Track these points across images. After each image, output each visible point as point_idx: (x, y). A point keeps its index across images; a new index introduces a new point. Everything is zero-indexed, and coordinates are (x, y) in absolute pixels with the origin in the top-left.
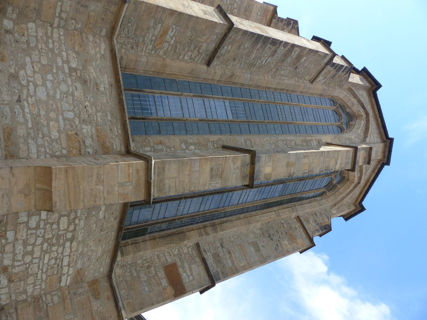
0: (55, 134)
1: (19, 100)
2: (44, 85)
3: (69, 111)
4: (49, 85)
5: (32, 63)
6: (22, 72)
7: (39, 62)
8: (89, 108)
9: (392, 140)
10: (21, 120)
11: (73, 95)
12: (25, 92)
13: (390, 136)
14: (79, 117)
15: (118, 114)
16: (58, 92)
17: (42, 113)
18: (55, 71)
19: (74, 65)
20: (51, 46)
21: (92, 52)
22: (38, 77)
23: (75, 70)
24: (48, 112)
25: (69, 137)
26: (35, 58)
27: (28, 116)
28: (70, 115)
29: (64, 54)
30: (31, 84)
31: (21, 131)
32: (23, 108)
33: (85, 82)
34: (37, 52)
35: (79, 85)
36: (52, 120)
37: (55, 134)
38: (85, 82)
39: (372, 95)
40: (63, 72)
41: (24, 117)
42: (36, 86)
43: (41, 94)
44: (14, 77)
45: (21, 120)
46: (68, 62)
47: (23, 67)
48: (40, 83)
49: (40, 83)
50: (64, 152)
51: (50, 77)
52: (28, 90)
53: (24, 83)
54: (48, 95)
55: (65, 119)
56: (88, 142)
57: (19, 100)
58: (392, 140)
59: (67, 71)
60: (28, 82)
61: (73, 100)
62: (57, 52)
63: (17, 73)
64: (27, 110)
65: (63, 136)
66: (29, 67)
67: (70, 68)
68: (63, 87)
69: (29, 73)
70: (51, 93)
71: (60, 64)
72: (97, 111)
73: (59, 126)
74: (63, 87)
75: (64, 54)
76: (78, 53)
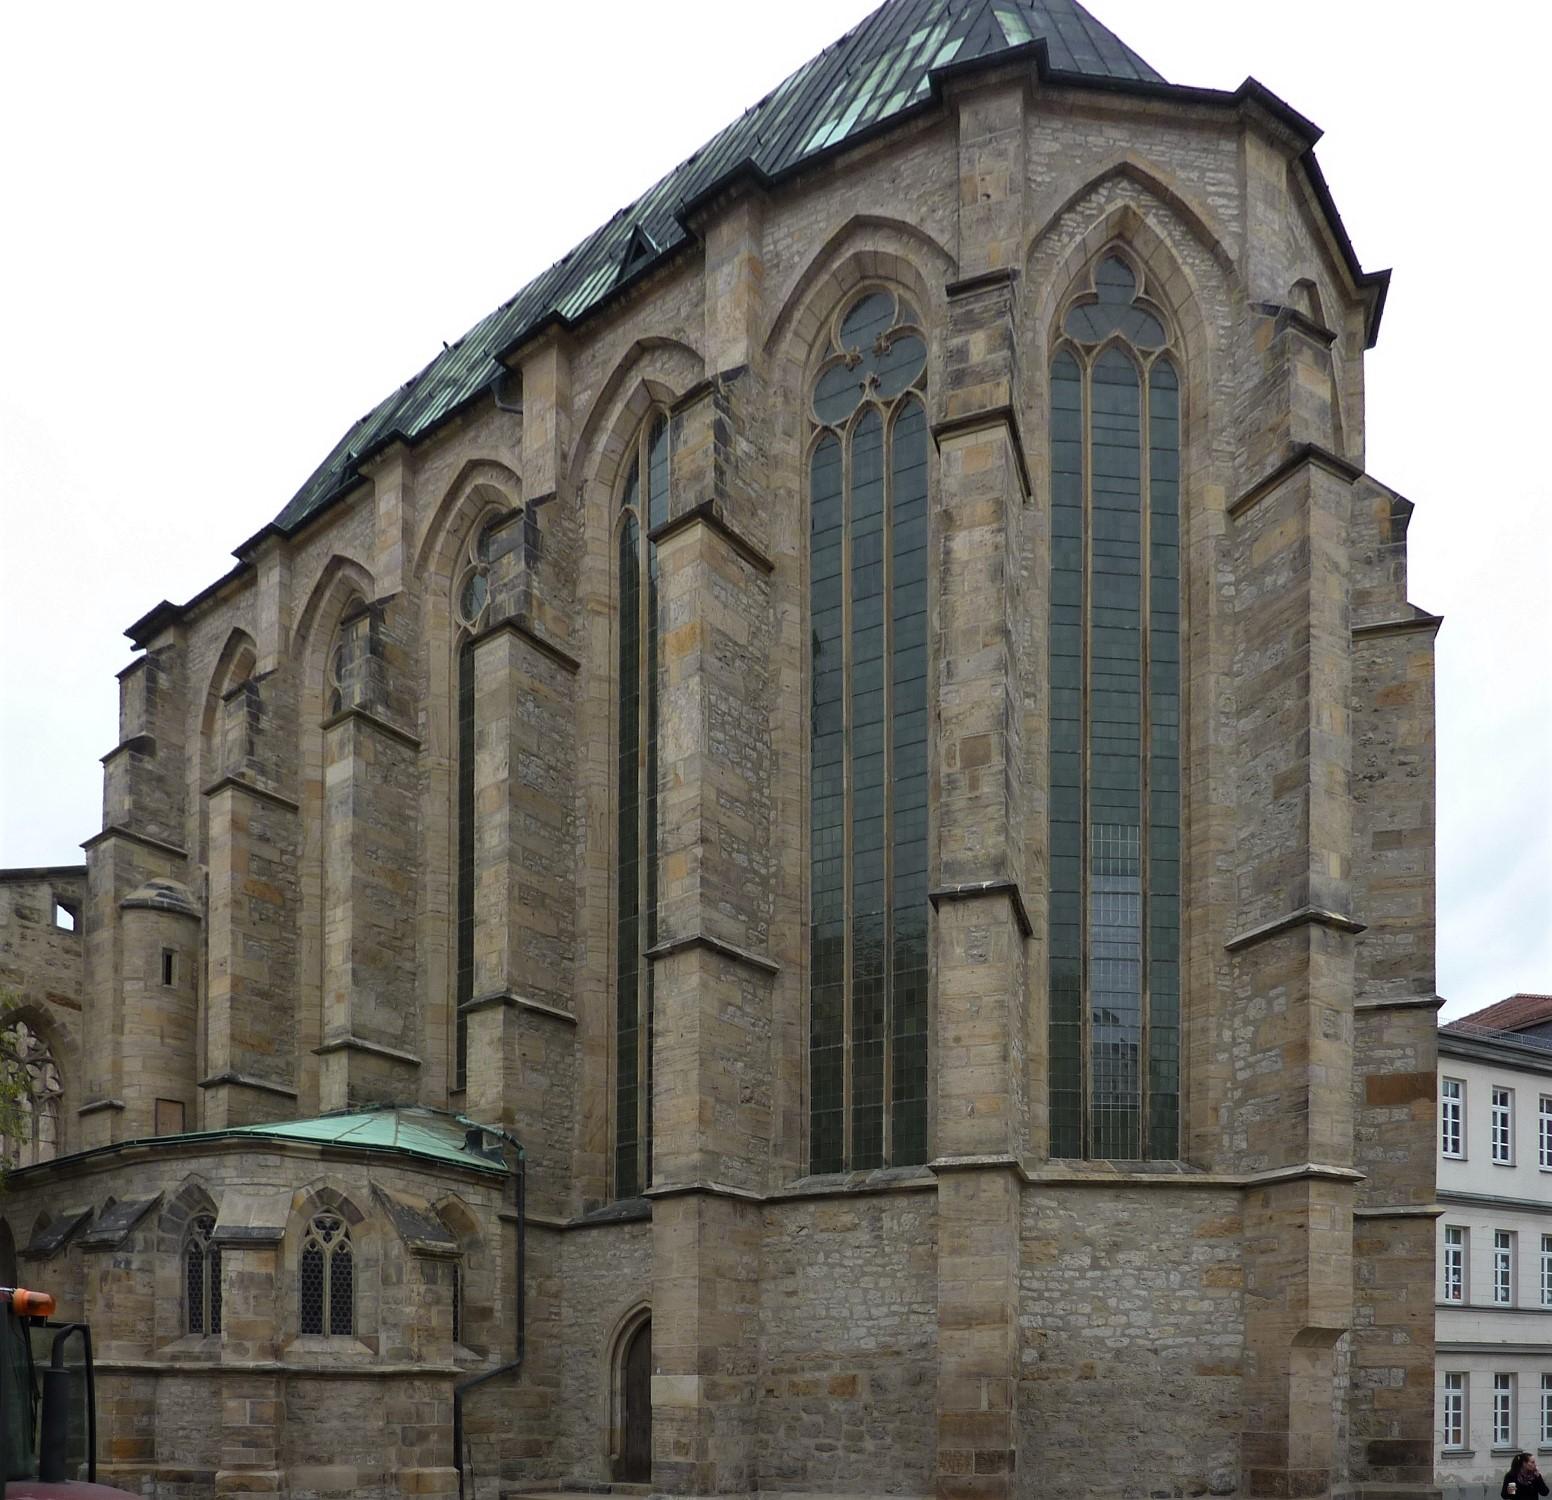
0: (1207, 1305)
1: (1155, 1352)
2: (1126, 1313)
3: (1168, 1279)
4: (1128, 1305)
5: (1090, 1326)
6: (1109, 1343)
7: (1089, 1316)
8: (1164, 1246)
9: (1251, 88)
10: (1185, 1350)
11: (1140, 1269)
12: (1140, 1341)
13: (1231, 84)
14: (1179, 1264)
15: (1173, 1195)
16: (1136, 1292)
17: (1172, 1320)
18: (1101, 1294)
19: (1087, 1261)
20: (1056, 1295)
21: (1055, 1225)
22: (1113, 1320)
23: (1095, 1259)
24: (1171, 1312)
25: (1211, 1285)
26: (1083, 1321)
27: (1179, 1340)
28: (1175, 1278)
29: (1068, 1274)
30: (1127, 1332)
31: (1203, 1353)
32: (1167, 1347)
33: (1116, 1247)
34: (1072, 1318)
35: (1121, 1257)
36: (1184, 1307)
37: (1207, 1305)
38: (1115, 1244)
39: (1054, 95)
40: (1102, 1279)
41: (1180, 1346)
42: (1129, 1325)
43: (1142, 1318)
44: (1118, 1354)
45: (1185, 1350)
46: (1082, 1270)
47: (1101, 1341)
48: (1123, 1319)
49: (1123, 1319)
50: (1235, 1294)
51: (1112, 1302)
52: (1137, 1336)
53: (1126, 1341)
54: (1143, 1309)
55: (1182, 1287)
56: (1221, 1254)
57: (1155, 1352)
58: (1251, 88)
59: (1098, 1273)
60: (1124, 1335)
61: (1149, 1270)
62: (1066, 1286)
63: (1110, 1350)
64: (1170, 1342)
65: (1210, 1292)
66: (1099, 1332)
67: (1095, 1266)
68: (1129, 1282)
69: (1108, 1332)
70: (1139, 1303)
71: (1088, 1283)
72: (1167, 1232)
73: (1194, 1297)
74: (1129, 1282)
75: (1068, 1274)
76: (1063, 1252)
